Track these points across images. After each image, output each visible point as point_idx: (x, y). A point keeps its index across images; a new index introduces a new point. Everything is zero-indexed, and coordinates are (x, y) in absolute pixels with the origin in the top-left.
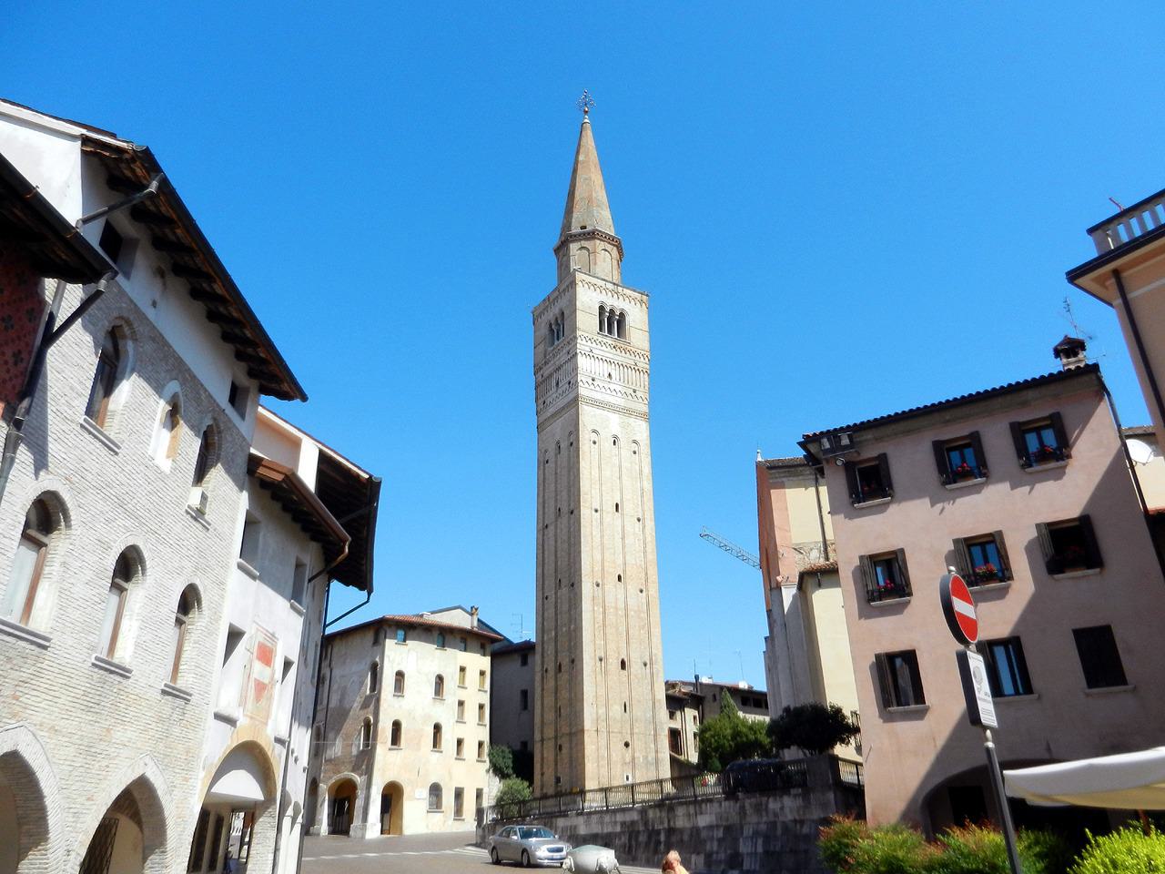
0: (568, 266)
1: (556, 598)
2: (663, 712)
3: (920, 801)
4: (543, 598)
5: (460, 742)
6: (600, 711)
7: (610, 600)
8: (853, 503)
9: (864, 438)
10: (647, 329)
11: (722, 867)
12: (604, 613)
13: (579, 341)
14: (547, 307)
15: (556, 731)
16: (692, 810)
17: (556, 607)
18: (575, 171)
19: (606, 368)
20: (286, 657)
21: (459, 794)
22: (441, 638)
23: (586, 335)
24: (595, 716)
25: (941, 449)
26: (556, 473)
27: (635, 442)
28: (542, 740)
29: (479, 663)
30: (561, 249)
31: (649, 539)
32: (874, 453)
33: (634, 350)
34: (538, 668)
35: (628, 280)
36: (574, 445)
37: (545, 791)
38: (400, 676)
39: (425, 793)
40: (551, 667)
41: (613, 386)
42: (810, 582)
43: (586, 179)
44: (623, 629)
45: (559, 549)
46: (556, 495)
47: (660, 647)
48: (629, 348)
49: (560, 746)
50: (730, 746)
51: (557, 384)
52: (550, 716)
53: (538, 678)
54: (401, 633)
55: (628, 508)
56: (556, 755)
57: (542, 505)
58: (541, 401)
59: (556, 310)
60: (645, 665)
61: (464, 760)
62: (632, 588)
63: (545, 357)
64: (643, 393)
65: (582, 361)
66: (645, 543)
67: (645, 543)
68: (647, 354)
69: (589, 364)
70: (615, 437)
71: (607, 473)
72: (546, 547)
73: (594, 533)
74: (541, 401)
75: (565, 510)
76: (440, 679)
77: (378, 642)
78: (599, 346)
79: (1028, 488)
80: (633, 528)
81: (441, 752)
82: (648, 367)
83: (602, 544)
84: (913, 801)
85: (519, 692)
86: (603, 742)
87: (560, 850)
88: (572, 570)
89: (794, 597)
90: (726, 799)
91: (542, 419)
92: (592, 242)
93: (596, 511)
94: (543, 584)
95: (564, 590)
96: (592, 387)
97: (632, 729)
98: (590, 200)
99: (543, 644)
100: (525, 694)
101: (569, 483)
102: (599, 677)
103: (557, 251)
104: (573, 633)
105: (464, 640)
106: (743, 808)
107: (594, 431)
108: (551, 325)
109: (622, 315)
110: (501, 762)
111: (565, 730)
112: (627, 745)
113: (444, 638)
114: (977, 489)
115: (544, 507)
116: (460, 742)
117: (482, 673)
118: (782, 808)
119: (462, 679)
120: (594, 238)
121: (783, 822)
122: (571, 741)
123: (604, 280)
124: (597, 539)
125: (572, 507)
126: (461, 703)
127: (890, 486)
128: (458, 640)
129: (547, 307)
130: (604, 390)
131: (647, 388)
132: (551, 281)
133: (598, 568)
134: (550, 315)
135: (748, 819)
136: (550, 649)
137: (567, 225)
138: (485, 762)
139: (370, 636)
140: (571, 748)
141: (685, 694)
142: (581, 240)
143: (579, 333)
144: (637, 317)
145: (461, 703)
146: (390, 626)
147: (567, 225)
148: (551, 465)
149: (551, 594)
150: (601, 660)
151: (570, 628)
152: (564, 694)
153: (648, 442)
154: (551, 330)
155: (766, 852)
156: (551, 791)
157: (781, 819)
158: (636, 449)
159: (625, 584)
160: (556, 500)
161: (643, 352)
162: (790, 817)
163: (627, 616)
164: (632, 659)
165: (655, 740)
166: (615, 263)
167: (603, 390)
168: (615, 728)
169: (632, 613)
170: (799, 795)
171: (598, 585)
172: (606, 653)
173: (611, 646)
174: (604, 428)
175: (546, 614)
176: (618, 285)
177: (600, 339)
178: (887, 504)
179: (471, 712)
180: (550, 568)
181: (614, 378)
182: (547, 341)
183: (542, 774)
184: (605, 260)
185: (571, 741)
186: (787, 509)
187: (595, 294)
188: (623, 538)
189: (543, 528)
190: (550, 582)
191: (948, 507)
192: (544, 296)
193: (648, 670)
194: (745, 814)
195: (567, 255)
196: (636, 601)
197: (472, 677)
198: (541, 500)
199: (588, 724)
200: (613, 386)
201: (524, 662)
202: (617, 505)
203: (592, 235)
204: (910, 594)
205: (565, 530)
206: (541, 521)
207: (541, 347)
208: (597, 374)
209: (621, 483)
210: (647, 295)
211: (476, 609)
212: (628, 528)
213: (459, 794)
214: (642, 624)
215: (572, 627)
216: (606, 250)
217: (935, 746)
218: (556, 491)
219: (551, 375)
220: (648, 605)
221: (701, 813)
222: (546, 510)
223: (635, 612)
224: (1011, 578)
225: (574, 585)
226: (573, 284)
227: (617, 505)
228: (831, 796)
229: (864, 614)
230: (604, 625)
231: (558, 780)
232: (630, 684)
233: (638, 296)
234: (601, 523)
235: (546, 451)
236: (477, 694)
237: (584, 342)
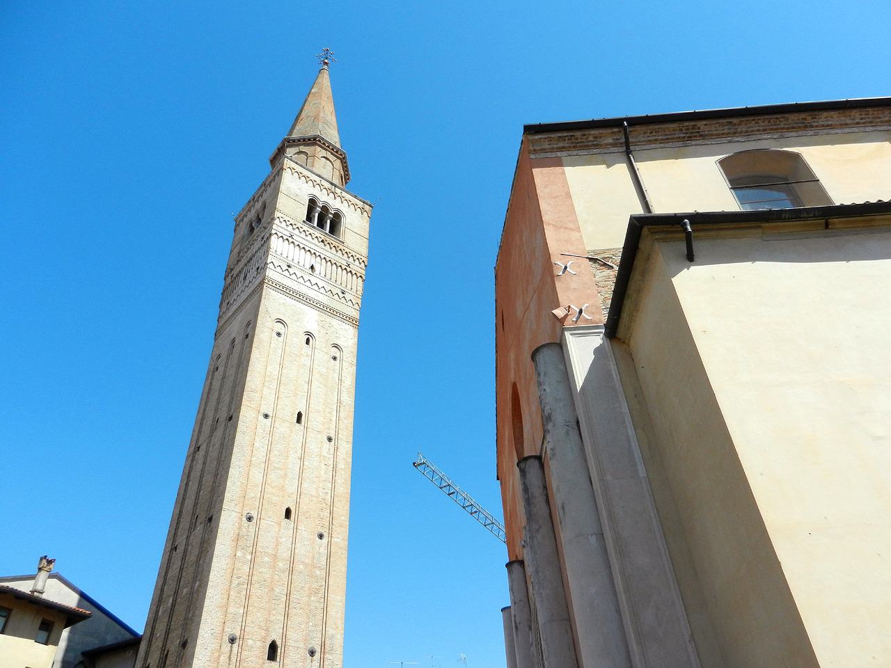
1: (187, 545)
7: (266, 542)
10: (367, 237)
12: (253, 561)
13: (277, 221)
17: (183, 559)
19: (309, 260)
27: (336, 346)
31: (341, 465)
33: (347, 250)
41: (314, 280)
44: (280, 590)
47: (341, 624)
48: (341, 247)
55: (314, 419)
57: (201, 422)
59: (258, 205)
60: (312, 653)
62: (306, 527)
63: (239, 255)
65: (275, 243)
66: (334, 468)
67: (334, 468)
68: (364, 259)
70: (309, 334)
73: (257, 444)
74: (225, 304)
75: (223, 415)
78: (303, 235)
80: (317, 445)
82: (364, 272)
83: (267, 461)
89: (598, 351)
91: (221, 324)
92: (312, 148)
93: (266, 416)
94: (176, 529)
95: (199, 528)
98: (316, 118)
107: (280, 321)
108: (251, 224)
124: (261, 454)
131: (360, 293)
133: (254, 493)
134: (252, 215)
136: (160, 633)
142: (300, 145)
143: (277, 214)
144: (355, 223)
150: (232, 640)
153: (355, 351)
158: (338, 355)
159: (296, 522)
160: (216, 410)
161: (362, 257)
163: (291, 571)
164: (290, 643)
169: (301, 566)
171: (250, 519)
172: (243, 630)
173: (256, 617)
175: (169, 575)
176: (335, 186)
177: (305, 228)
180: (189, 503)
181: (317, 271)
184: (328, 168)
186: (568, 196)
187: (305, 185)
188: (302, 459)
192: (250, 196)
200: (314, 280)
202: (300, 415)
206: (194, 443)
207: (236, 250)
208: (296, 261)
210: (370, 206)
211: (50, 562)
212: (312, 446)
214: (315, 586)
220: (329, 556)
223: (306, 565)
225: (211, 521)
227: (300, 415)
230: (250, 583)
233: (361, 204)
235: (219, 357)
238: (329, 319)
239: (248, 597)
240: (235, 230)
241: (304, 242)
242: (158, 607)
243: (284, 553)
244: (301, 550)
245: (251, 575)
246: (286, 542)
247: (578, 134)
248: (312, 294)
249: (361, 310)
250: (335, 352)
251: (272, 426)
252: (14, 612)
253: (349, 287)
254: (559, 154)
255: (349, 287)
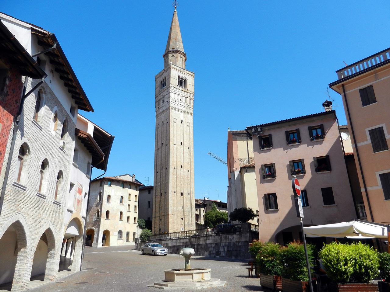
0: (168, 62)
1: (161, 172)
2: (194, 209)
3: (275, 236)
4: (156, 172)
5: (128, 217)
6: (174, 209)
8: (261, 149)
9: (265, 129)
11: (214, 255)
12: (176, 178)
13: (171, 88)
14: (160, 75)
15: (160, 214)
16: (205, 238)
17: (161, 175)
18: (171, 28)
20: (85, 192)
21: (128, 233)
22: (123, 184)
23: (173, 86)
24: (172, 210)
25: (288, 133)
26: (162, 132)
27: (188, 122)
28: (155, 217)
29: (136, 192)
30: (166, 56)
32: (268, 134)
34: (154, 195)
35: (188, 68)
36: (168, 122)
37: (155, 233)
38: (109, 196)
39: (117, 233)
40: (159, 194)
41: (181, 104)
42: (244, 170)
43: (175, 32)
44: (182, 183)
45: (162, 157)
46: (162, 139)
48: (187, 91)
49: (161, 219)
50: (215, 219)
51: (163, 102)
52: (158, 210)
53: (154, 197)
54: (109, 183)
55: (185, 144)
56: (159, 223)
58: (157, 107)
59: (163, 77)
60: (189, 194)
61: (130, 223)
62: (186, 170)
63: (159, 93)
64: (191, 106)
69: (174, 96)
70: (182, 120)
71: (179, 132)
72: (158, 156)
73: (174, 152)
74: (157, 107)
75: (165, 144)
76: (122, 197)
77: (101, 185)
78: (178, 90)
79: (312, 146)
80: (186, 150)
81: (122, 221)
83: (176, 156)
84: (273, 236)
85: (148, 202)
86: (175, 218)
87: (164, 250)
88: (167, 164)
90: (216, 235)
91: (157, 113)
93: (175, 145)
94: (157, 168)
95: (164, 170)
96: (175, 104)
97: (184, 214)
98: (176, 39)
99: (156, 187)
100: (149, 202)
101: (166, 135)
102: (174, 198)
103: (164, 56)
104: (166, 184)
105: (130, 185)
106: (221, 238)
108: (161, 81)
109: (185, 80)
110: (141, 224)
111: (163, 214)
112: (182, 219)
113: (124, 185)
114: (297, 146)
115: (157, 143)
116: (128, 217)
117: (136, 196)
118: (233, 238)
119: (130, 198)
120: (177, 53)
121: (233, 242)
122: (164, 218)
123: (180, 68)
125: (167, 143)
126: (129, 205)
127: (272, 144)
128: (128, 185)
129: (160, 75)
130: (179, 105)
132: (162, 67)
133: (175, 163)
134: (161, 79)
135: (223, 241)
136: (158, 189)
137: (168, 47)
138: (136, 224)
139: (99, 184)
140: (164, 220)
141: (201, 203)
142: (172, 53)
143: (171, 85)
144: (190, 81)
145: (129, 205)
146: (106, 180)
147: (168, 47)
148: (160, 129)
149: (159, 171)
150: (175, 192)
151: (165, 182)
152: (163, 203)
154: (162, 84)
155: (228, 251)
156: (157, 233)
157: (233, 241)
160: (162, 141)
162: (235, 241)
165: (191, 217)
166: (184, 61)
167: (178, 105)
168: (179, 213)
169: (185, 178)
170: (238, 234)
171: (175, 169)
173: (178, 188)
174: (178, 117)
175: (157, 178)
176: (184, 70)
177: (178, 88)
178: (271, 149)
179: (132, 208)
180: (159, 163)
181: (182, 101)
182: (160, 87)
183: (155, 228)
184: (180, 61)
185: (164, 218)
186: (237, 147)
189: (157, 149)
190: (159, 168)
191: (289, 151)
192: (160, 71)
193: (190, 196)
194: (222, 240)
195: (168, 58)
196: (187, 174)
197: (133, 197)
198: (156, 140)
199: (170, 212)
200: (181, 104)
201: (149, 193)
203: (176, 52)
204: (276, 177)
205: (164, 151)
207: (158, 89)
209: (183, 136)
210: (194, 74)
211: (134, 175)
212: (185, 151)
213: (128, 233)
215: (166, 182)
216: (181, 57)
217: (280, 221)
218: (162, 138)
219: (161, 99)
220: (191, 175)
221: (208, 240)
222: (158, 143)
224: (305, 173)
225: (167, 169)
226: (169, 68)
228: (248, 234)
229: (262, 182)
231: (160, 229)
232: (184, 200)
234: (176, 149)
236: (134, 202)
237: (173, 88)
238: (186, 115)
239: (176, 184)
240: (156, 81)
241: (178, 92)
242: (156, 183)
243: (182, 175)
244: (185, 174)
245: (176, 180)
246: (182, 173)
247: (240, 135)
248: (181, 108)
249: (193, 110)
250: (188, 124)
251: (176, 147)
252: (132, 185)
253: (190, 103)
254: (237, 138)
255: (190, 103)
